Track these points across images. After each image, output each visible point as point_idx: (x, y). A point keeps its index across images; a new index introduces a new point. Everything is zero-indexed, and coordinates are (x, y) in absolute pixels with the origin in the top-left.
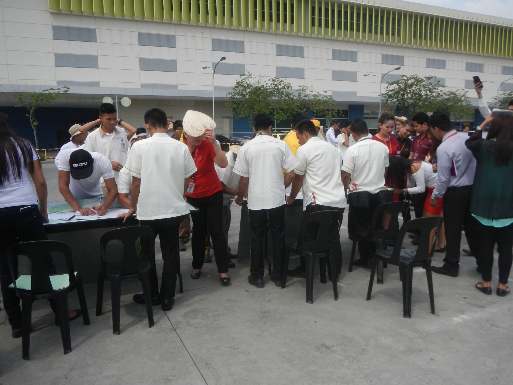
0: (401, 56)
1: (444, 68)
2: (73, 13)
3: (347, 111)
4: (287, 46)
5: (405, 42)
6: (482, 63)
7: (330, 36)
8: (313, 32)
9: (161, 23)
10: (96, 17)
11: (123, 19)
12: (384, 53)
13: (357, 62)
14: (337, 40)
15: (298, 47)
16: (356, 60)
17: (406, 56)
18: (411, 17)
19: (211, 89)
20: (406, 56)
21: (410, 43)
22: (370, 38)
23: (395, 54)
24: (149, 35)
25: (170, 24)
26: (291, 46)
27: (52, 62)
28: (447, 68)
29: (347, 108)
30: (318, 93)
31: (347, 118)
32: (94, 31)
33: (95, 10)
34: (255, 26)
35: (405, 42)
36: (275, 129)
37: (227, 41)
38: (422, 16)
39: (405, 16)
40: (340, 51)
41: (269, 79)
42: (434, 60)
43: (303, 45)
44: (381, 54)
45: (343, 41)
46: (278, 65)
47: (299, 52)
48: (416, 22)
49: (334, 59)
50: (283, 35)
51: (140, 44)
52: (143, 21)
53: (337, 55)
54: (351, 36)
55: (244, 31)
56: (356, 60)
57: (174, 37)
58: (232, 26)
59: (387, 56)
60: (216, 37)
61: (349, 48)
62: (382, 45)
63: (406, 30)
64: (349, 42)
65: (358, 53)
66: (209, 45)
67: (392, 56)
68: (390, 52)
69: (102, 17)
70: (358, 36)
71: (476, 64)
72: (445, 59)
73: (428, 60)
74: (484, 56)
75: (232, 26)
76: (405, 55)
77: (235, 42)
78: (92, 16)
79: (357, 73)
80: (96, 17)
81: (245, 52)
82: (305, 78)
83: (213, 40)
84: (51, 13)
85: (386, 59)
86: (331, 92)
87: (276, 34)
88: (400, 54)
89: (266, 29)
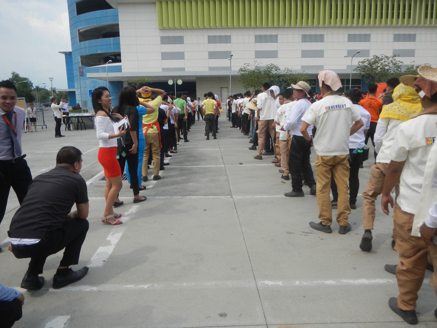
0: (412, 34)
2: (171, 28)
5: (414, 22)
9: (222, 28)
10: (184, 29)
11: (198, 29)
12: (396, 33)
14: (351, 27)
24: (215, 37)
25: (227, 28)
27: (160, 57)
30: (296, 72)
32: (183, 37)
33: (182, 25)
35: (414, 22)
37: (266, 36)
40: (355, 35)
41: (267, 65)
43: (323, 33)
44: (393, 35)
45: (357, 27)
47: (320, 39)
49: (349, 40)
50: (307, 27)
51: (209, 42)
52: (210, 28)
55: (278, 28)
56: (369, 41)
57: (230, 36)
62: (394, 27)
64: (362, 27)
66: (253, 39)
69: (187, 29)
77: (271, 36)
78: (181, 29)
80: (184, 29)
81: (279, 41)
82: (325, 56)
84: (160, 29)
87: (301, 28)
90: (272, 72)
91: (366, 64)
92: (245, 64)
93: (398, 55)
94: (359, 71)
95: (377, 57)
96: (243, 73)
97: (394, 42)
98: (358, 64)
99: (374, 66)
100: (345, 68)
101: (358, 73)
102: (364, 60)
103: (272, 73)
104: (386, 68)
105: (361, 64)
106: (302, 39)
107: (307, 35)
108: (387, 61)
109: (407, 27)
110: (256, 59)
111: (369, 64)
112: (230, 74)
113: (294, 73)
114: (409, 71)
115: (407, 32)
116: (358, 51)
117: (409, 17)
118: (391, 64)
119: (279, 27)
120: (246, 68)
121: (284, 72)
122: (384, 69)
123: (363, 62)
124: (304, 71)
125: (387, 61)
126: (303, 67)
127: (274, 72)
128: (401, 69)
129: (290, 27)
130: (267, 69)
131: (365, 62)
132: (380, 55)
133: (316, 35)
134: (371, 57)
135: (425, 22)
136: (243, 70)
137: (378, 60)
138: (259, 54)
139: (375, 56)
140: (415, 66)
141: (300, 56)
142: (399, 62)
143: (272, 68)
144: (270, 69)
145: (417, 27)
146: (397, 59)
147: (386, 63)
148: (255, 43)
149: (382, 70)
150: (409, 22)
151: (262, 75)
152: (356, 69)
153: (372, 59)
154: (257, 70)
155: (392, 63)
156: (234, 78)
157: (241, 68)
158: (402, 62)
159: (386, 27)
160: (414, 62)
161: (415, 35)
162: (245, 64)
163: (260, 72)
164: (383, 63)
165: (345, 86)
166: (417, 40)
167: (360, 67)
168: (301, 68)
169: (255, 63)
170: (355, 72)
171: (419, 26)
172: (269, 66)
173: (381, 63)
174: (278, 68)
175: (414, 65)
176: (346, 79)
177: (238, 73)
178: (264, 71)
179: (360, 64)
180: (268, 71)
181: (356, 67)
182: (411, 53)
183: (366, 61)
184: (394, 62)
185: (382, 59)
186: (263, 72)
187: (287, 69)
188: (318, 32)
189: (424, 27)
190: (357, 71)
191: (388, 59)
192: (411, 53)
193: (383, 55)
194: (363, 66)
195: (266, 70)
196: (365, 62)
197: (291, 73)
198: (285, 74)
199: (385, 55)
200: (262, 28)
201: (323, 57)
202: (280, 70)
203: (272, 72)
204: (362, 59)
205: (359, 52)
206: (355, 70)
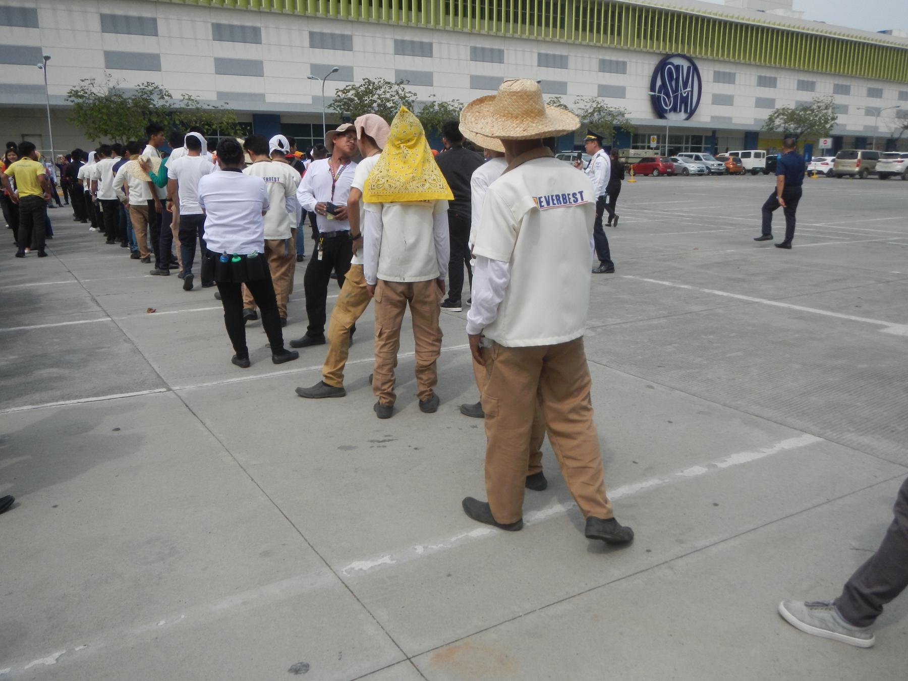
0: (426, 43)
1: (501, 61)
4: (231, 27)
5: (428, 21)
6: (565, 53)
12: (399, 37)
13: (352, 51)
14: (315, 18)
16: (350, 49)
21: (437, 21)
23: (417, 39)
28: (505, 61)
30: (208, 105)
35: (428, 21)
37: (127, 18)
40: (322, 35)
42: (483, 49)
43: (258, 25)
44: (393, 40)
45: (326, 19)
47: (253, 36)
49: (312, 45)
50: (221, 8)
53: (317, 41)
56: (351, 49)
59: (403, 42)
62: (393, 26)
64: (336, 20)
65: (353, 37)
66: (95, 23)
67: (412, 42)
68: (408, 36)
71: (554, 56)
72: (502, 48)
74: (567, 44)
77: (141, 19)
81: (160, 33)
82: (266, 74)
83: (103, 17)
86: (311, 97)
88: (426, 39)
90: (152, 104)
91: (351, 94)
92: (82, 81)
93: (407, 80)
94: (338, 109)
95: (369, 82)
96: (80, 101)
97: (395, 54)
98: (336, 94)
99: (366, 100)
100: (310, 101)
101: (337, 112)
102: (347, 86)
103: (154, 105)
104: (389, 105)
105: (341, 96)
108: (389, 91)
109: (417, 28)
110: (109, 71)
111: (357, 95)
112: (47, 103)
113: (205, 107)
114: (427, 113)
115: (418, 37)
116: (335, 68)
117: (419, 9)
118: (397, 97)
120: (86, 91)
121: (181, 103)
122: (385, 107)
123: (345, 91)
124: (228, 104)
125: (388, 92)
126: (220, 95)
127: (158, 103)
128: (413, 108)
130: (140, 94)
131: (348, 91)
132: (376, 79)
133: (243, 28)
134: (358, 81)
135: (446, 23)
136: (79, 94)
137: (372, 88)
138: (114, 60)
139: (367, 79)
140: (436, 104)
141: (213, 71)
142: (410, 95)
143: (151, 93)
144: (147, 94)
145: (434, 30)
146: (408, 88)
147: (388, 96)
149: (382, 109)
150: (418, 19)
151: (129, 108)
152: (334, 104)
153: (361, 86)
154: (115, 95)
155: (399, 96)
156: (58, 113)
157: (75, 89)
158: (415, 94)
159: (378, 24)
160: (434, 96)
161: (431, 44)
162: (82, 81)
163: (124, 102)
164: (382, 95)
165: (312, 138)
167: (340, 101)
168: (218, 98)
169: (108, 79)
170: (331, 111)
171: (437, 28)
172: (142, 87)
173: (378, 94)
174: (167, 94)
175: (435, 102)
176: (313, 125)
177: (67, 100)
178: (133, 100)
179: (340, 93)
180: (143, 99)
181: (333, 100)
182: (426, 79)
183: (350, 89)
184: (401, 94)
185: (380, 87)
186: (130, 101)
187: (187, 97)
189: (444, 31)
190: (335, 109)
191: (391, 88)
192: (426, 79)
193: (381, 78)
194: (346, 99)
195: (139, 98)
196: (349, 92)
197: (199, 106)
198: (183, 108)
199: (384, 80)
201: (261, 75)
202: (169, 96)
203: (152, 102)
204: (342, 85)
205: (336, 70)
206: (330, 106)
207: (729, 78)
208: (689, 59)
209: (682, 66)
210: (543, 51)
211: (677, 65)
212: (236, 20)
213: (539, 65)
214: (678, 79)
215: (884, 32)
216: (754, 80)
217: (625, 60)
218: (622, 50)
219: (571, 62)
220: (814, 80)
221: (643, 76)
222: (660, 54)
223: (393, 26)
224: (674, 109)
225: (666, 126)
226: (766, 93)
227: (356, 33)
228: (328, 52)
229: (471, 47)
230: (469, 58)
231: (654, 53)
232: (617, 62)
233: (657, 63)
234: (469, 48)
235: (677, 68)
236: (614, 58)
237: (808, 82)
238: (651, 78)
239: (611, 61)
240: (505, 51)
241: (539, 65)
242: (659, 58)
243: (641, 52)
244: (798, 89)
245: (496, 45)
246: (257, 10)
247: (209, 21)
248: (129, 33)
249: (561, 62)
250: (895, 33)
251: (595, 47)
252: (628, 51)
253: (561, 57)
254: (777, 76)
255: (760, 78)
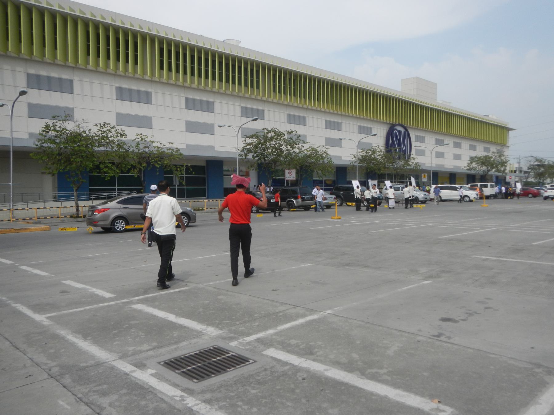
3: (205, 166)
6: (340, 121)
7: (181, 82)
8: (161, 76)
12: (243, 105)
14: (190, 88)
15: (144, 91)
17: (266, 110)
18: (269, 70)
19: (26, 136)
20: (266, 110)
21: (269, 96)
22: (227, 88)
26: (134, 90)
28: (307, 124)
29: (204, 164)
31: (205, 175)
34: (87, 63)
35: (264, 95)
36: (116, 187)
37: (49, 78)
38: (281, 69)
39: (264, 69)
40: (194, 100)
42: (294, 116)
43: (150, 90)
45: (198, 89)
46: (118, 111)
48: (274, 76)
49: (187, 108)
50: (124, 77)
53: (191, 104)
54: (206, 84)
58: (56, 60)
59: (246, 108)
60: (32, 71)
61: (205, 97)
62: (240, 97)
63: (266, 82)
64: (204, 91)
65: (214, 103)
67: (252, 109)
68: (249, 105)
70: (213, 85)
71: (334, 122)
72: (305, 116)
73: (289, 116)
75: (56, 60)
76: (265, 109)
77: (60, 80)
79: (215, 125)
81: (74, 93)
83: (29, 76)
85: (245, 112)
86: (185, 145)
88: (260, 108)
89: (102, 68)
100: (185, 147)
106: (117, 95)
107: (125, 89)
117: (258, 87)
119: (75, 68)
129: (96, 72)
133: (139, 92)
148: (28, 88)
161: (263, 111)
166: (265, 118)
188: (143, 87)
189: (272, 102)
200: (42, 62)
207: (421, 139)
208: (405, 128)
209: (402, 131)
210: (328, 119)
211: (399, 131)
212: (134, 86)
213: (326, 128)
214: (399, 140)
215: (484, 115)
216: (434, 142)
217: (372, 126)
218: (370, 120)
219: (343, 126)
220: (461, 142)
221: (381, 137)
222: (389, 124)
223: (240, 97)
224: (399, 158)
225: (430, 170)
226: (440, 149)
227: (216, 101)
228: (198, 113)
229: (287, 114)
230: (286, 122)
231: (386, 123)
232: (367, 128)
233: (388, 129)
234: (286, 114)
235: (399, 132)
236: (365, 125)
237: (458, 143)
238: (385, 138)
239: (364, 127)
240: (307, 118)
241: (326, 128)
242: (389, 126)
243: (380, 122)
244: (454, 147)
245: (302, 114)
246: (150, 79)
247: (114, 84)
248: (50, 90)
249: (337, 126)
250: (490, 116)
251: (356, 118)
252: (373, 121)
253: (338, 123)
254: (444, 139)
255: (437, 140)
